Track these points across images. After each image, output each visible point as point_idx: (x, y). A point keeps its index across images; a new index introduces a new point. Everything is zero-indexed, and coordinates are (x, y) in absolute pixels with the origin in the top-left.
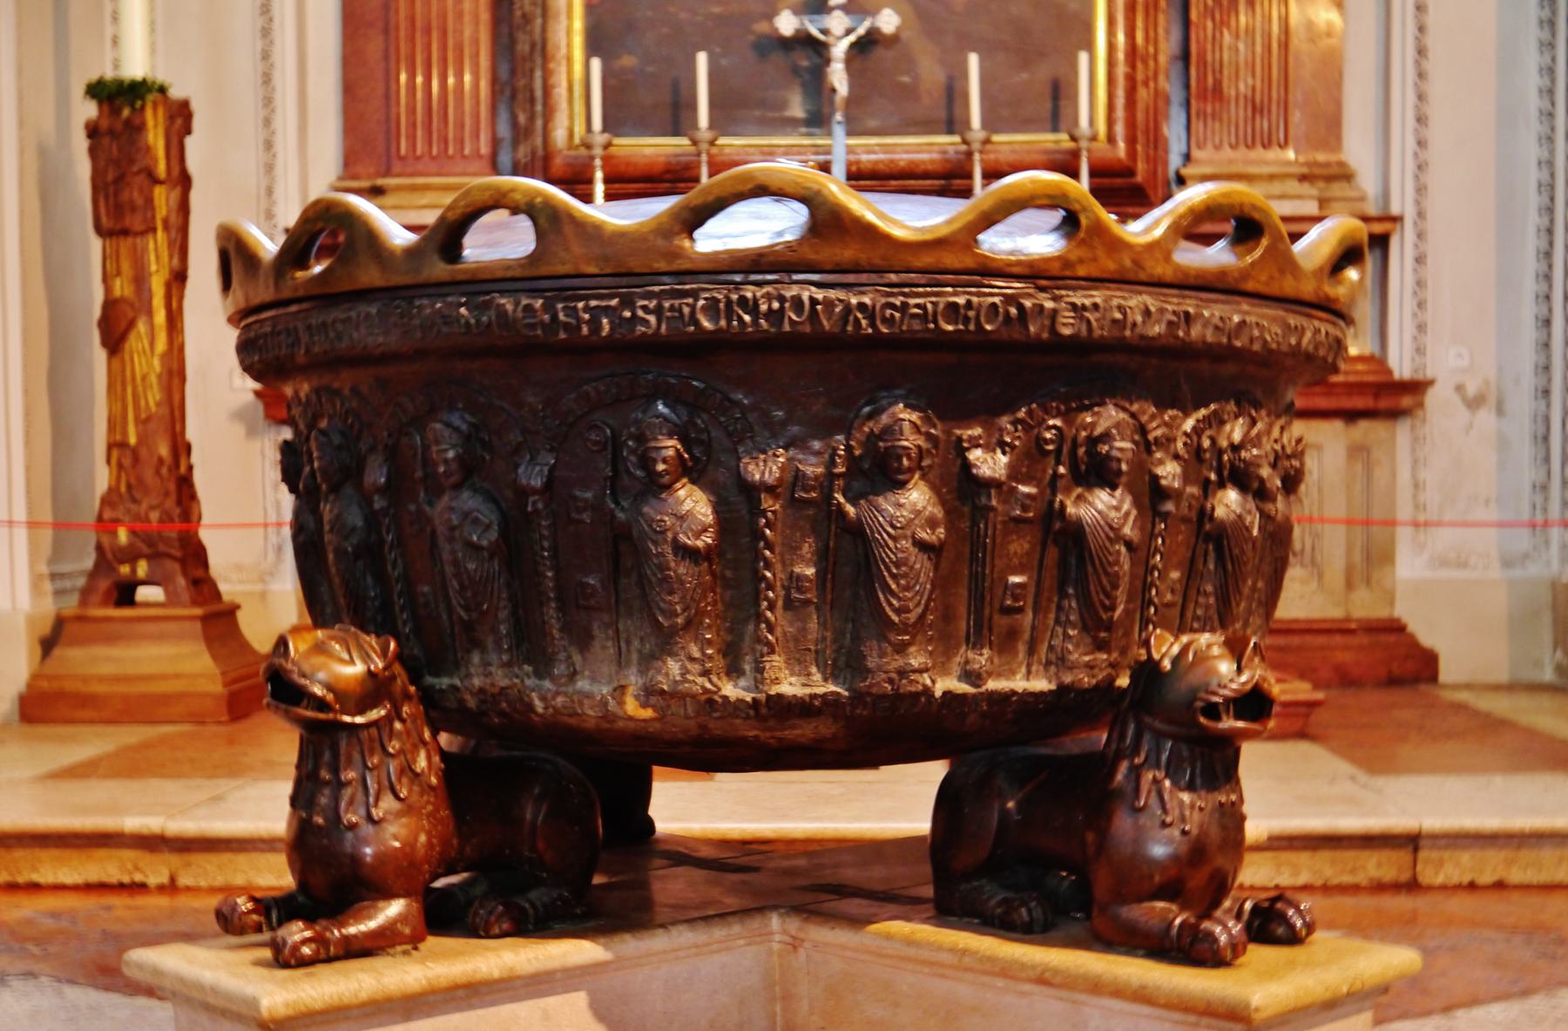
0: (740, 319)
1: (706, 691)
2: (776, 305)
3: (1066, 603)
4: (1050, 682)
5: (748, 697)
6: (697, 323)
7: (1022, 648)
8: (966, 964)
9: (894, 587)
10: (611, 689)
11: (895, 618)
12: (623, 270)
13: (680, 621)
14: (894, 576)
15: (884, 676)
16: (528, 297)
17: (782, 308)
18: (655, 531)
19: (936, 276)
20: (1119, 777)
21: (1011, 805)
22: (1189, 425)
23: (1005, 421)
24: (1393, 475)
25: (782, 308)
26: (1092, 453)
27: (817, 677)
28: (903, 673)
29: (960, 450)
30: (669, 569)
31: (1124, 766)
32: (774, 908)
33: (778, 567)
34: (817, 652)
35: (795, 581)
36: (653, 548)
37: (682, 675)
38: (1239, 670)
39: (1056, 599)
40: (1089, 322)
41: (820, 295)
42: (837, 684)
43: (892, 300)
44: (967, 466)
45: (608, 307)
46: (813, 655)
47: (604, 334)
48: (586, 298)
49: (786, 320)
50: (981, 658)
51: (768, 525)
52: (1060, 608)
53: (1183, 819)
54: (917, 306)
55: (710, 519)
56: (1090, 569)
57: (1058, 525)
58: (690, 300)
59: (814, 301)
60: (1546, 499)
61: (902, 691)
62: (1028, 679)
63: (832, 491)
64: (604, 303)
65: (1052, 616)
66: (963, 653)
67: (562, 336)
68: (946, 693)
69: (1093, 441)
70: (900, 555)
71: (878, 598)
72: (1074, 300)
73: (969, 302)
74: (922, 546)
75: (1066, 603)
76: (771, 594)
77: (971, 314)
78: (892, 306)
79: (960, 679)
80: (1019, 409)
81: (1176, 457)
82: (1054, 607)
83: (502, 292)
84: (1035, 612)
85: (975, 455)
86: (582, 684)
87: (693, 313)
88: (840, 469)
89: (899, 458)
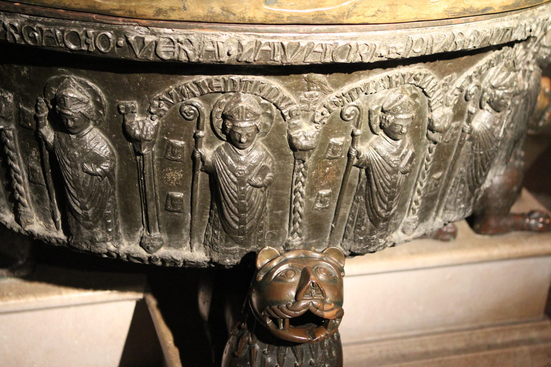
43: (31, 25)
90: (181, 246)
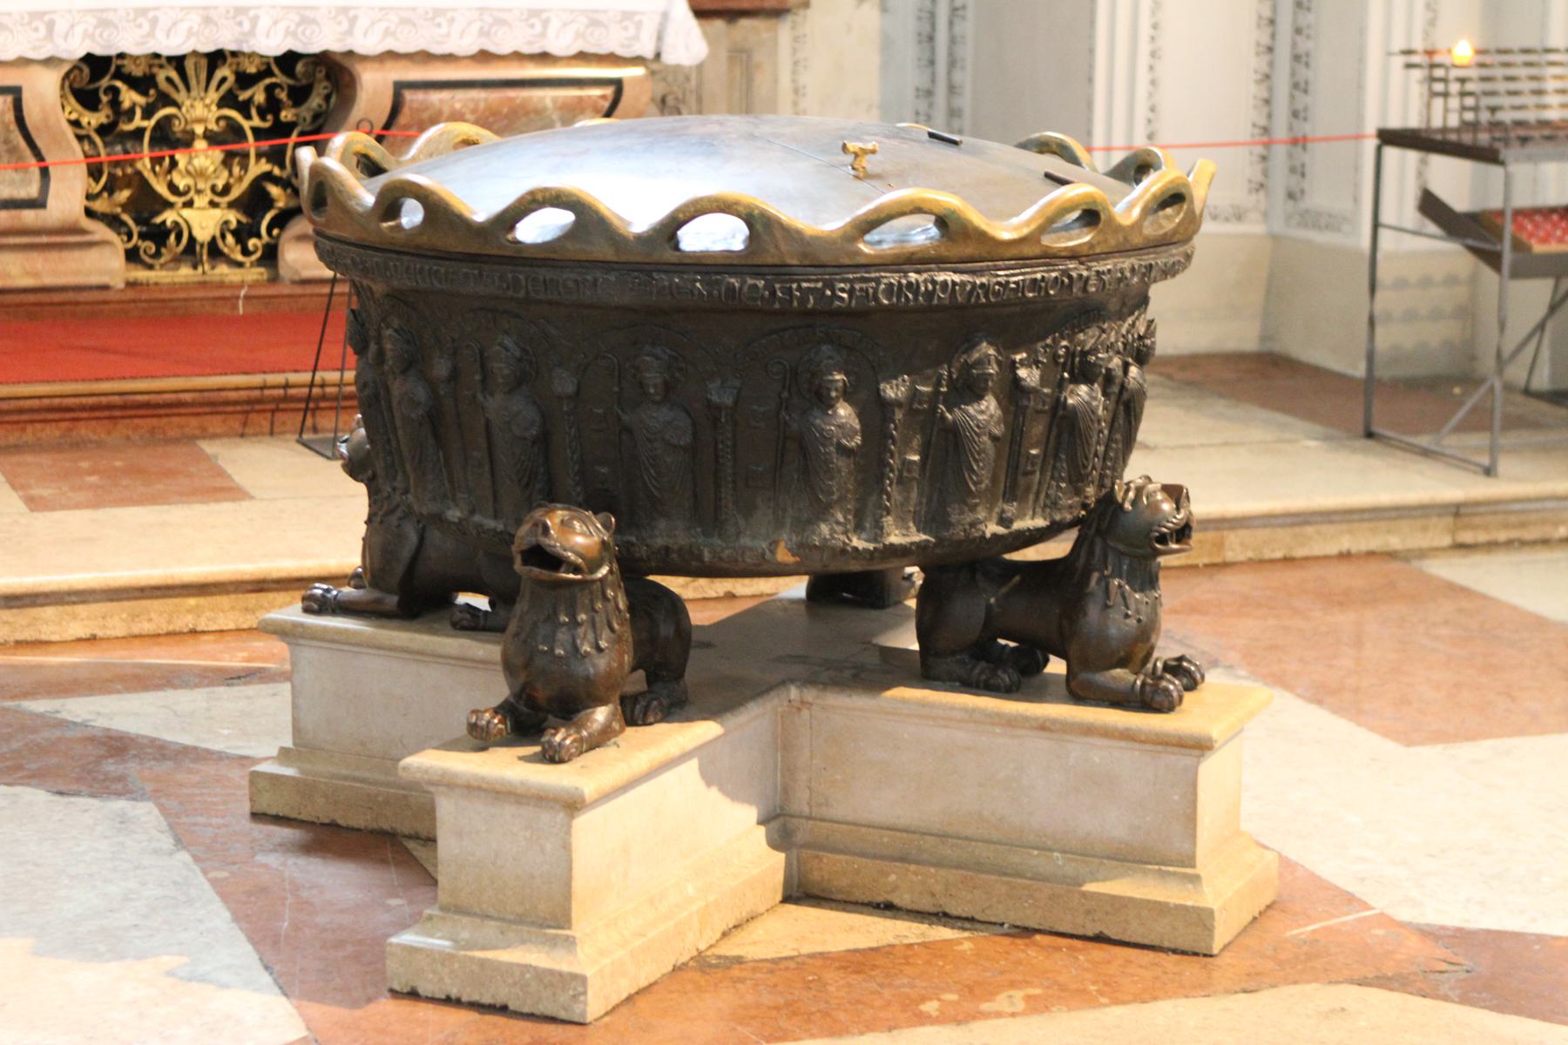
0: (906, 296)
1: (844, 543)
2: (930, 287)
3: (1058, 465)
4: (1045, 519)
5: (871, 546)
6: (876, 298)
7: (1032, 497)
8: (972, 714)
9: (975, 467)
10: (767, 543)
11: (973, 488)
12: (816, 263)
13: (835, 497)
14: (976, 461)
15: (961, 527)
16: (752, 278)
17: (934, 289)
18: (825, 437)
19: (1024, 260)
20: (1093, 583)
21: (992, 600)
22: (1124, 331)
23: (1039, 346)
24: (776, 81)
25: (934, 289)
26: (1085, 363)
27: (913, 529)
28: (973, 525)
29: (1013, 366)
30: (832, 463)
31: (1096, 576)
32: (792, 681)
33: (897, 456)
34: (915, 512)
35: (907, 465)
36: (822, 449)
37: (831, 535)
38: (1178, 509)
39: (1052, 462)
40: (1104, 283)
41: (957, 278)
42: (925, 533)
43: (999, 279)
44: (1017, 380)
45: (816, 288)
46: (912, 514)
47: (810, 306)
48: (798, 281)
49: (936, 297)
50: (1011, 509)
51: (895, 429)
52: (1054, 467)
53: (1138, 612)
54: (1015, 283)
55: (858, 427)
56: (1078, 441)
57: (1061, 413)
58: (874, 284)
59: (954, 283)
60: (931, 105)
61: (971, 537)
62: (1033, 519)
63: (937, 402)
64: (812, 285)
65: (1049, 474)
66: (1001, 505)
67: (777, 306)
68: (994, 535)
69: (1084, 354)
70: (982, 446)
71: (964, 475)
72: (1098, 268)
73: (1043, 277)
74: (994, 438)
75: (1058, 465)
76: (891, 475)
77: (1043, 284)
78: (999, 283)
79: (998, 524)
80: (1047, 337)
81: (1118, 352)
82: (1050, 467)
83: (731, 274)
84: (1041, 474)
85: (1022, 373)
86: (745, 541)
87: (875, 293)
88: (944, 389)
89: (987, 381)
90: (1025, 515)
